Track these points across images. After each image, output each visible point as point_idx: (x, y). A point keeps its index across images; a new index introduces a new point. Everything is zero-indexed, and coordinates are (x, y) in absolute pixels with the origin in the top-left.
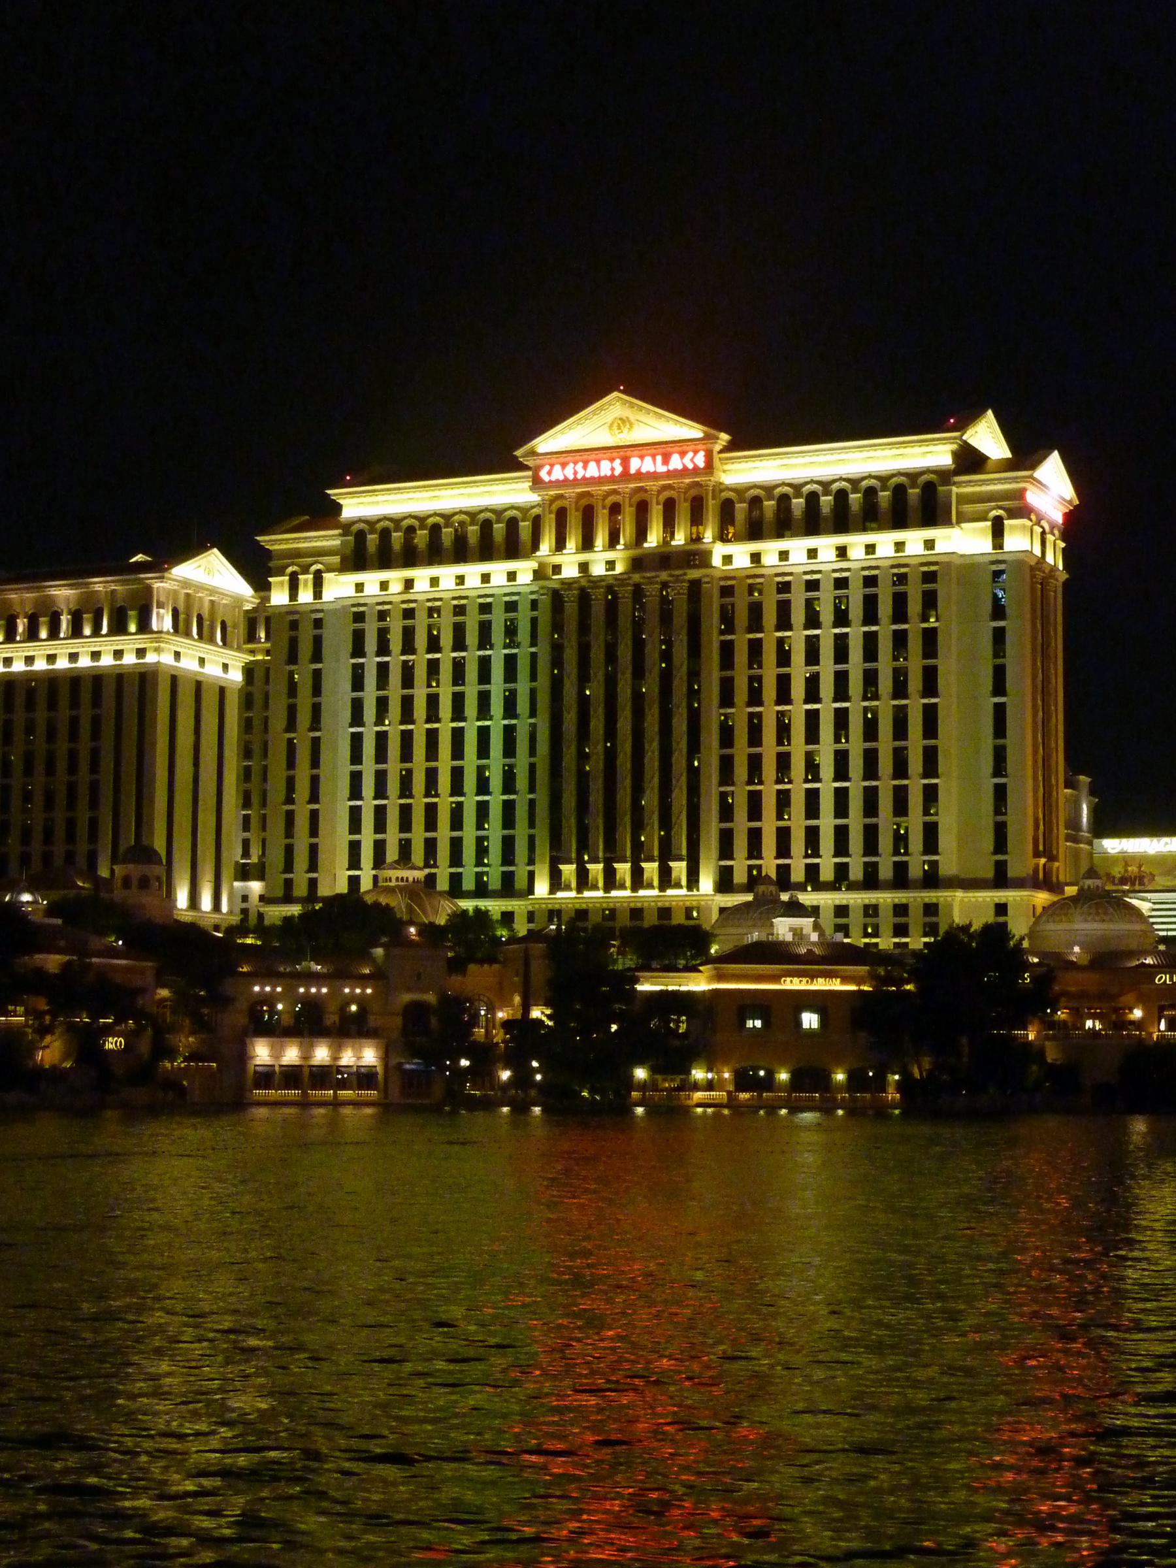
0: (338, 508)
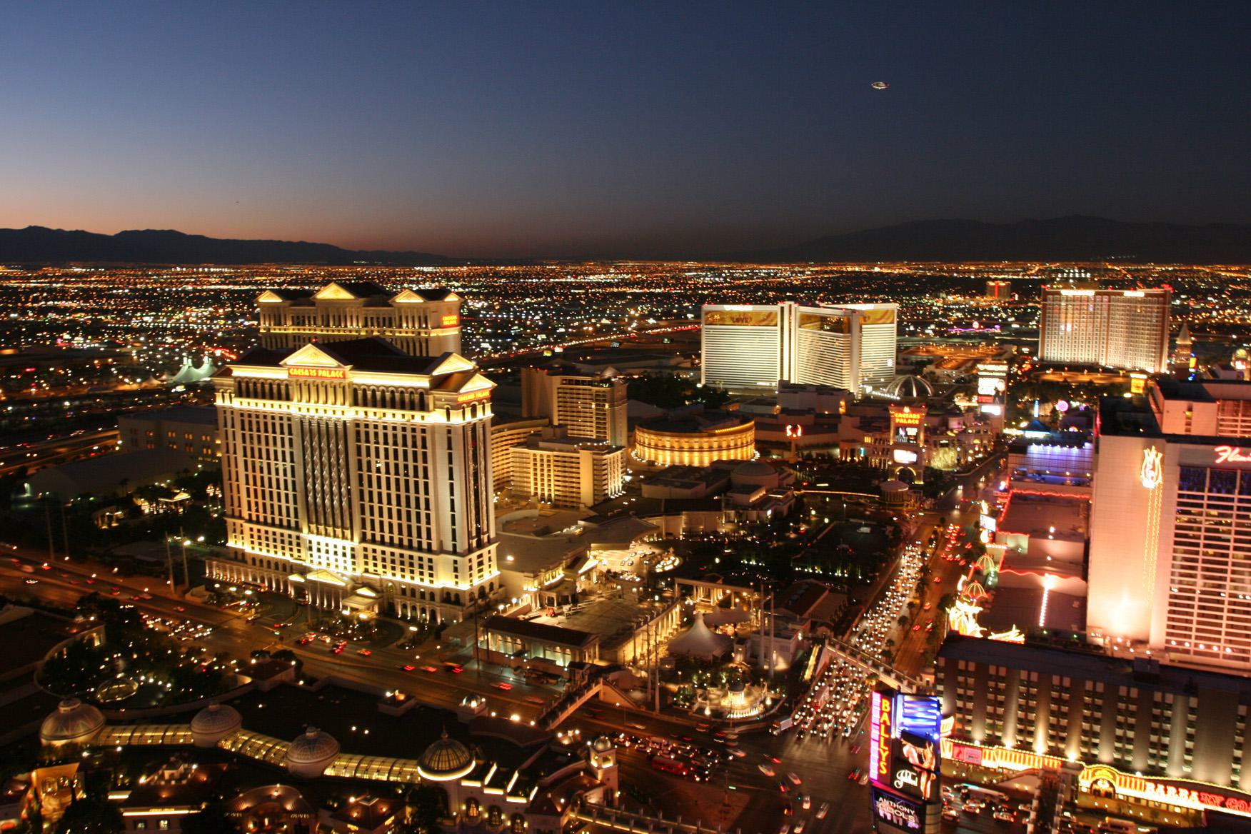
0: (231, 371)
